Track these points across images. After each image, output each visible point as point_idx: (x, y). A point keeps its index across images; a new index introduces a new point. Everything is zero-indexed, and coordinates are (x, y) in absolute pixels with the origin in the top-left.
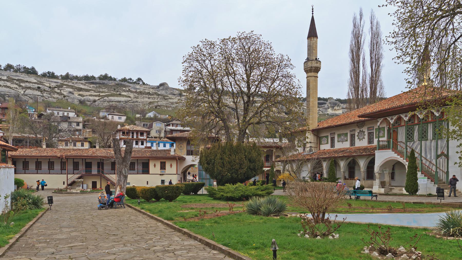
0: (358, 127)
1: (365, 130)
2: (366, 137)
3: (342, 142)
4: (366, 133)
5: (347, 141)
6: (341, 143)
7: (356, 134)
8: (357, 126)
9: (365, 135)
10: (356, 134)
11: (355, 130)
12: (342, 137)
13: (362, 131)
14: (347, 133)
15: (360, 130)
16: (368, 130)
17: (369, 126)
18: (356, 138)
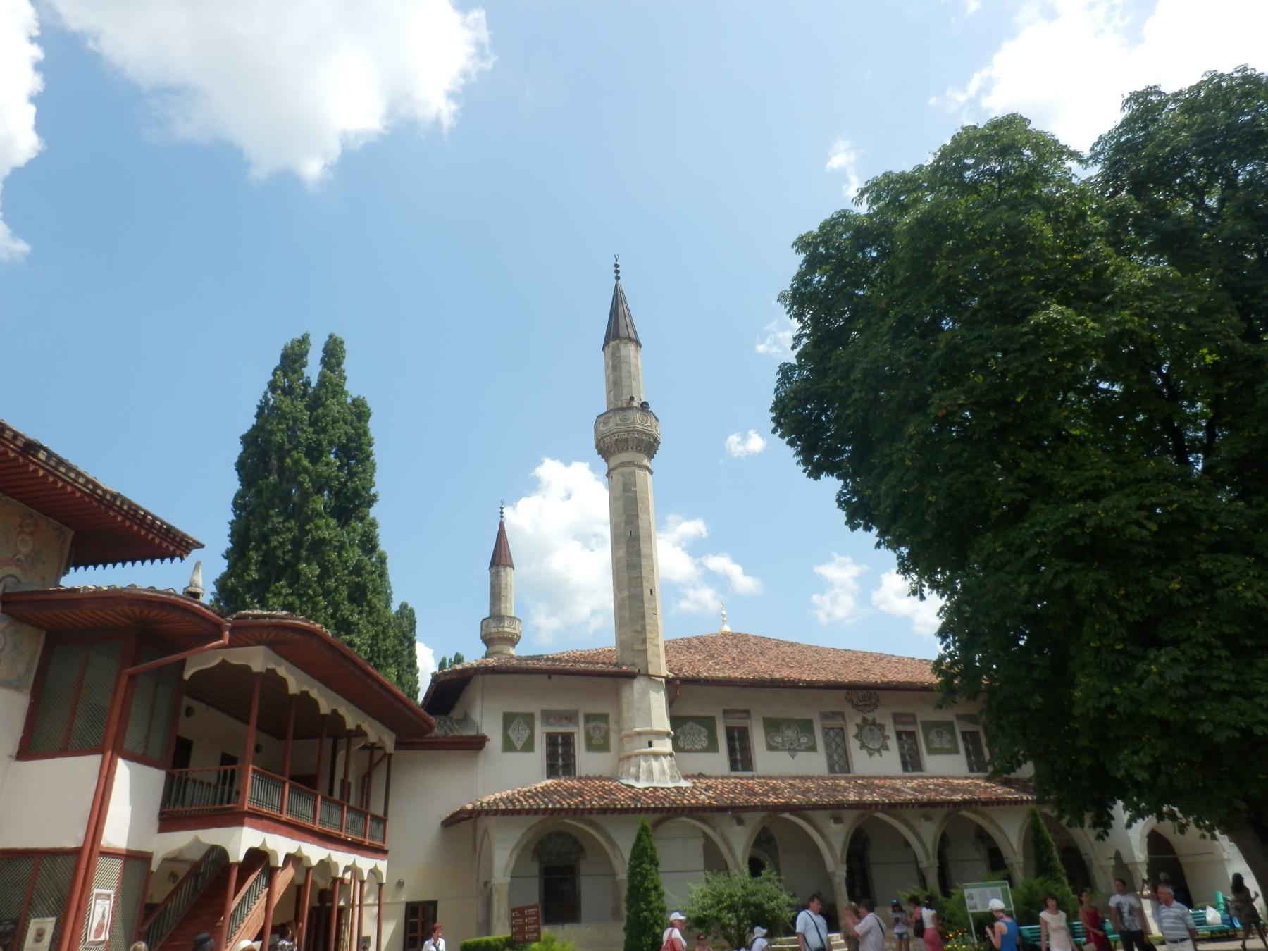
0: (855, 706)
1: (883, 716)
2: (893, 743)
3: (793, 751)
4: (890, 731)
5: (813, 748)
6: (785, 756)
7: (852, 730)
8: (850, 701)
9: (886, 738)
10: (852, 730)
11: (842, 714)
12: (790, 733)
13: (874, 723)
14: (810, 722)
15: (865, 720)
16: (896, 723)
17: (898, 710)
18: (854, 745)
